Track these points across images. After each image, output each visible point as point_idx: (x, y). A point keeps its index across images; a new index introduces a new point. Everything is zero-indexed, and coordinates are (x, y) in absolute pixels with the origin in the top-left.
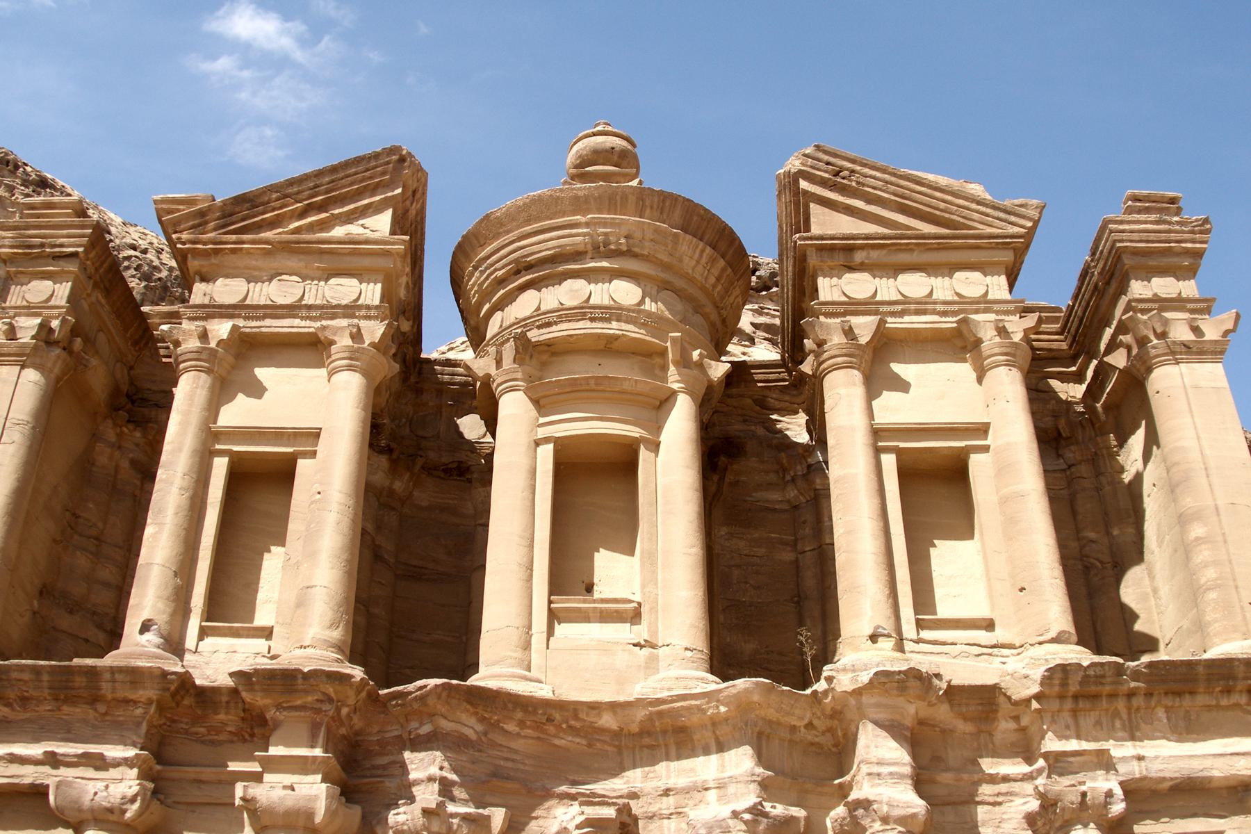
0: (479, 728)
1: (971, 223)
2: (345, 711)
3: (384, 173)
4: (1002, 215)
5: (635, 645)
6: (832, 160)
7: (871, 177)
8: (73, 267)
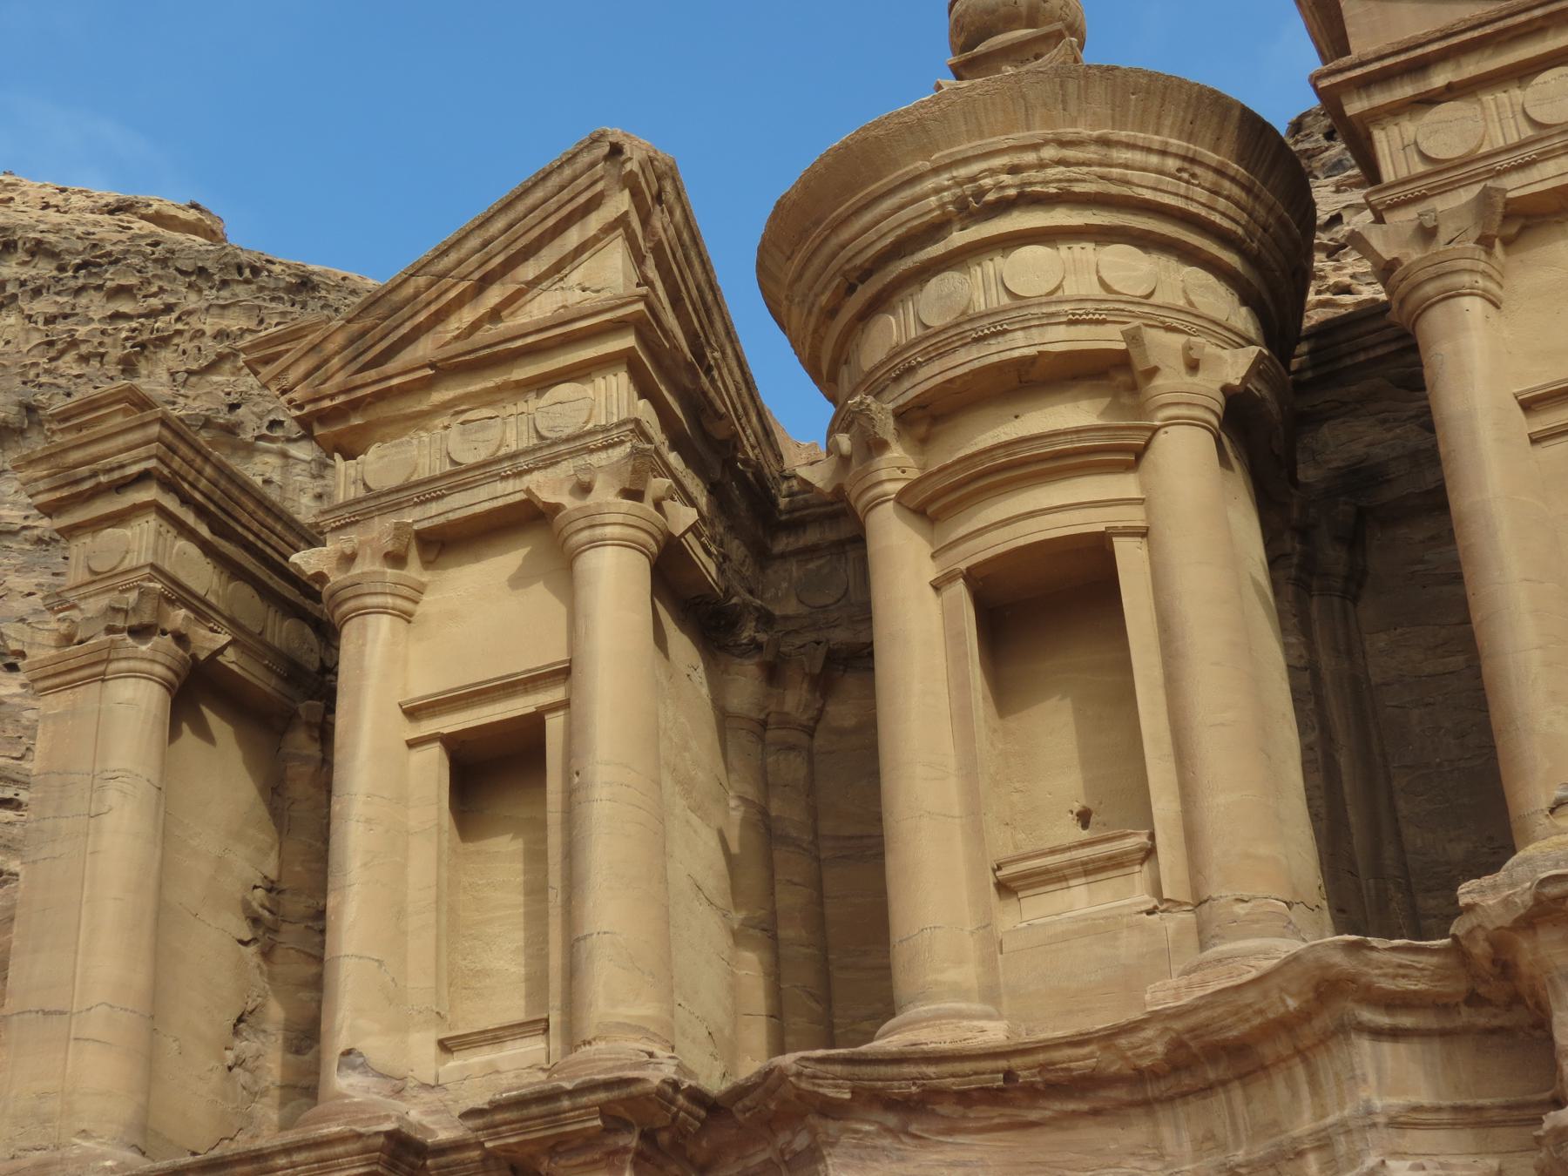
0: (892, 1120)
2: (664, 1138)
5: (1150, 912)
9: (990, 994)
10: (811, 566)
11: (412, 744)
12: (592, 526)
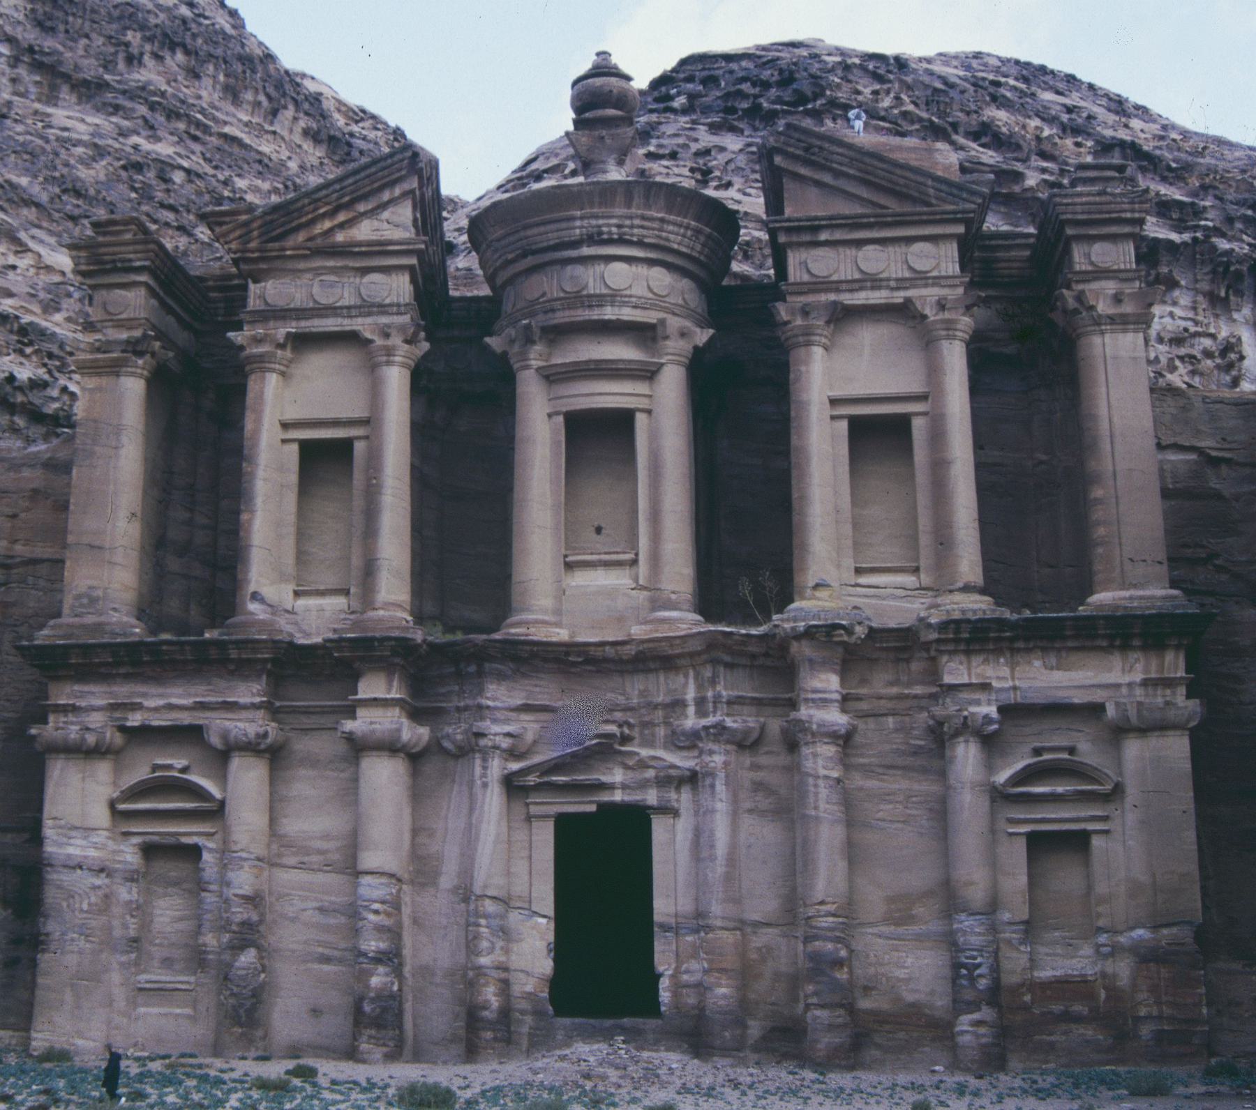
1: (926, 198)
4: (955, 191)
6: (803, 137)
7: (838, 154)
8: (143, 278)
9: (558, 612)
11: (284, 441)
12: (389, 355)
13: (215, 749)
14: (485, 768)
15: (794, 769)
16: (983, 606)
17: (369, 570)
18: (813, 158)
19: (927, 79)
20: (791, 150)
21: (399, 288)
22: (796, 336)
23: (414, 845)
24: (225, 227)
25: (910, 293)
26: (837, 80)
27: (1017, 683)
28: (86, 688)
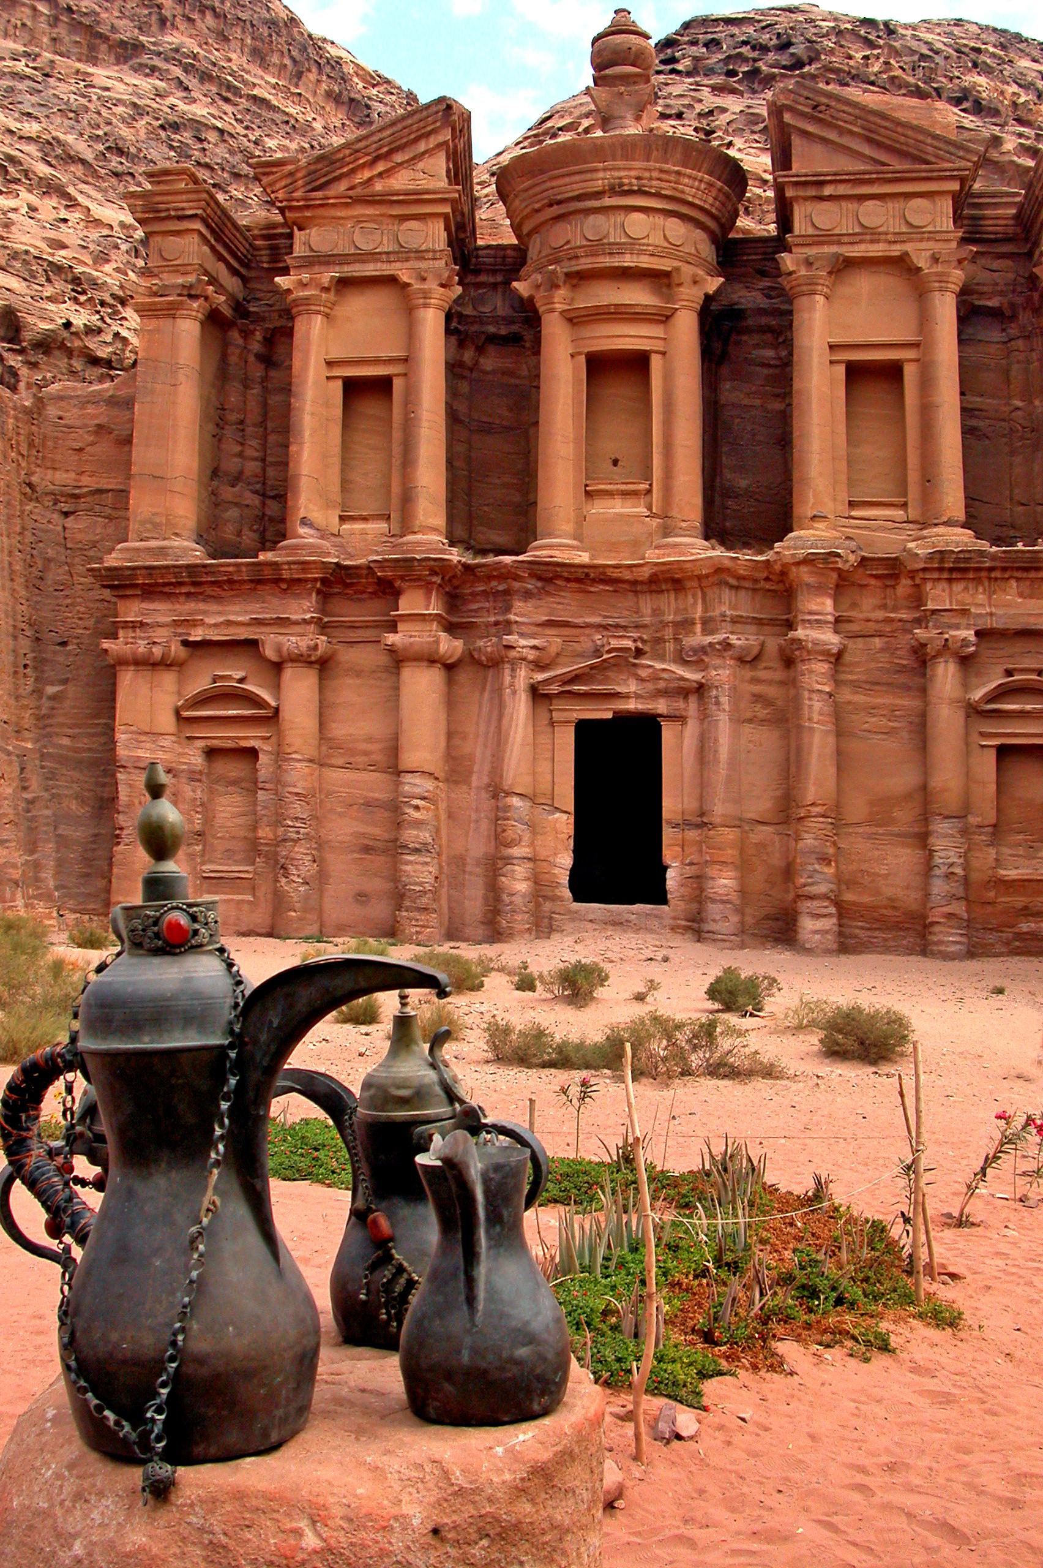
0: (539, 584)
3: (435, 122)
4: (952, 149)
6: (810, 95)
7: (844, 112)
10: (480, 291)
11: (328, 378)
12: (425, 298)
13: (270, 661)
14: (513, 677)
15: (791, 683)
16: (965, 539)
17: (407, 499)
18: (821, 115)
19: (914, 44)
20: (800, 107)
21: (435, 236)
22: (799, 285)
23: (448, 747)
24: (271, 177)
25: (908, 247)
26: (831, 45)
27: (993, 610)
28: (152, 606)
